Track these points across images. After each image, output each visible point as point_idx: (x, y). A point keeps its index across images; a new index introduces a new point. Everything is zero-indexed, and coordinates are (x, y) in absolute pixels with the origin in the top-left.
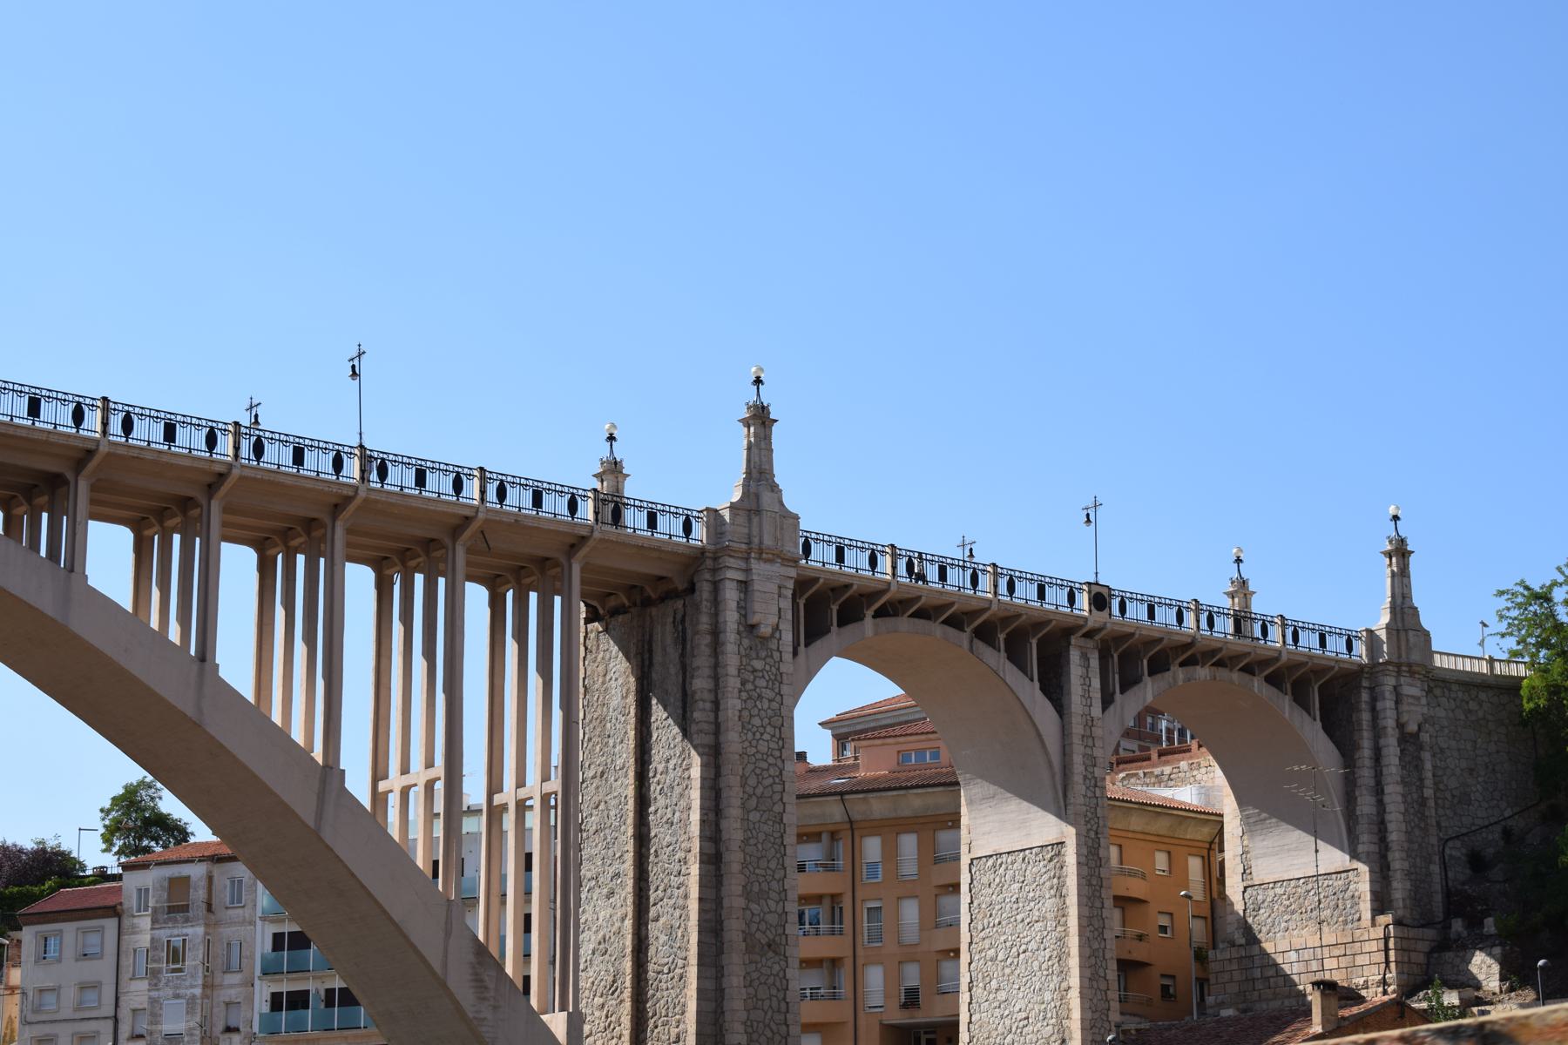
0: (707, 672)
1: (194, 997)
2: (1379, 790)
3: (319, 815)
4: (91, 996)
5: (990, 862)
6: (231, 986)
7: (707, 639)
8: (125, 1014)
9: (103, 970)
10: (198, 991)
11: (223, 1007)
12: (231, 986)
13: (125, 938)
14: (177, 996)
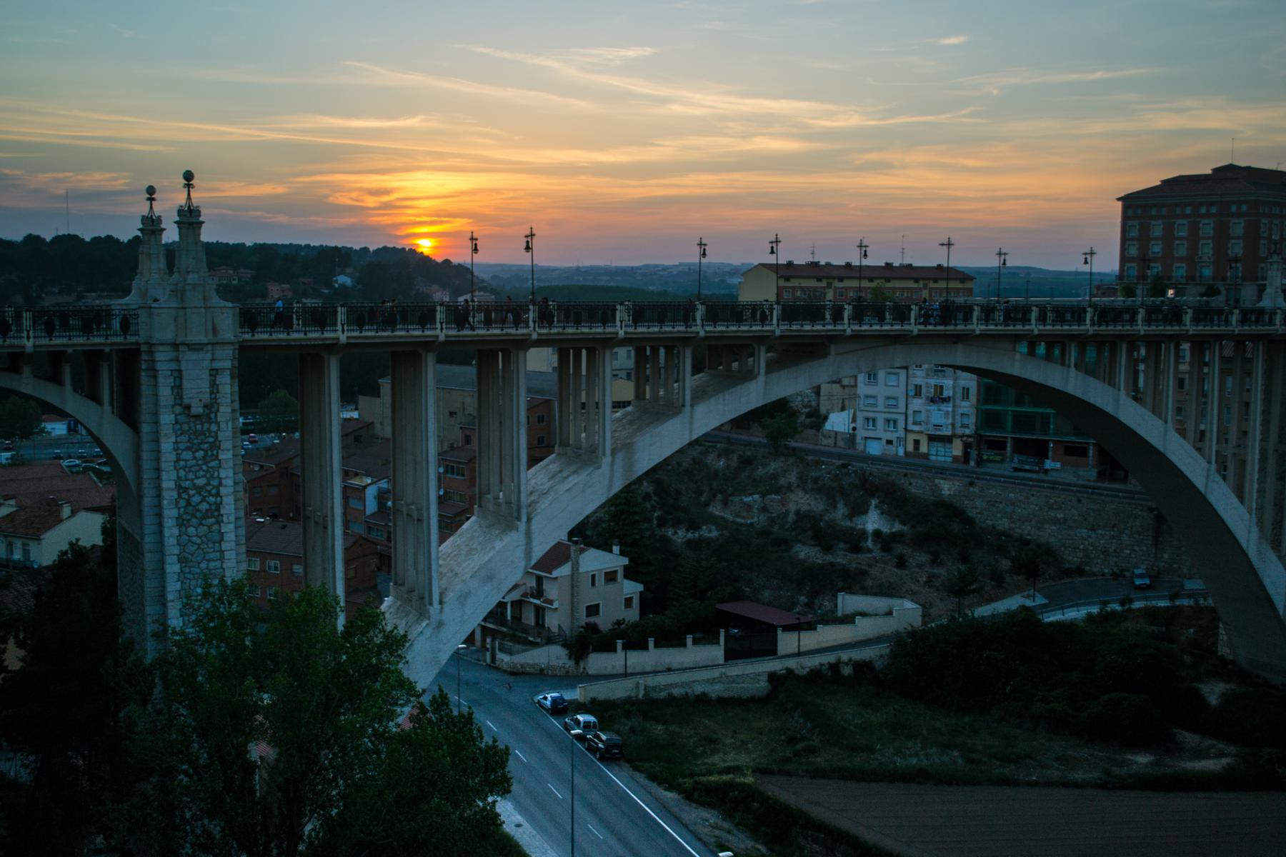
1: (948, 412)
3: (1206, 487)
6: (964, 407)
8: (910, 412)
9: (900, 392)
10: (950, 409)
11: (960, 415)
12: (964, 407)
13: (910, 379)
14: (939, 410)
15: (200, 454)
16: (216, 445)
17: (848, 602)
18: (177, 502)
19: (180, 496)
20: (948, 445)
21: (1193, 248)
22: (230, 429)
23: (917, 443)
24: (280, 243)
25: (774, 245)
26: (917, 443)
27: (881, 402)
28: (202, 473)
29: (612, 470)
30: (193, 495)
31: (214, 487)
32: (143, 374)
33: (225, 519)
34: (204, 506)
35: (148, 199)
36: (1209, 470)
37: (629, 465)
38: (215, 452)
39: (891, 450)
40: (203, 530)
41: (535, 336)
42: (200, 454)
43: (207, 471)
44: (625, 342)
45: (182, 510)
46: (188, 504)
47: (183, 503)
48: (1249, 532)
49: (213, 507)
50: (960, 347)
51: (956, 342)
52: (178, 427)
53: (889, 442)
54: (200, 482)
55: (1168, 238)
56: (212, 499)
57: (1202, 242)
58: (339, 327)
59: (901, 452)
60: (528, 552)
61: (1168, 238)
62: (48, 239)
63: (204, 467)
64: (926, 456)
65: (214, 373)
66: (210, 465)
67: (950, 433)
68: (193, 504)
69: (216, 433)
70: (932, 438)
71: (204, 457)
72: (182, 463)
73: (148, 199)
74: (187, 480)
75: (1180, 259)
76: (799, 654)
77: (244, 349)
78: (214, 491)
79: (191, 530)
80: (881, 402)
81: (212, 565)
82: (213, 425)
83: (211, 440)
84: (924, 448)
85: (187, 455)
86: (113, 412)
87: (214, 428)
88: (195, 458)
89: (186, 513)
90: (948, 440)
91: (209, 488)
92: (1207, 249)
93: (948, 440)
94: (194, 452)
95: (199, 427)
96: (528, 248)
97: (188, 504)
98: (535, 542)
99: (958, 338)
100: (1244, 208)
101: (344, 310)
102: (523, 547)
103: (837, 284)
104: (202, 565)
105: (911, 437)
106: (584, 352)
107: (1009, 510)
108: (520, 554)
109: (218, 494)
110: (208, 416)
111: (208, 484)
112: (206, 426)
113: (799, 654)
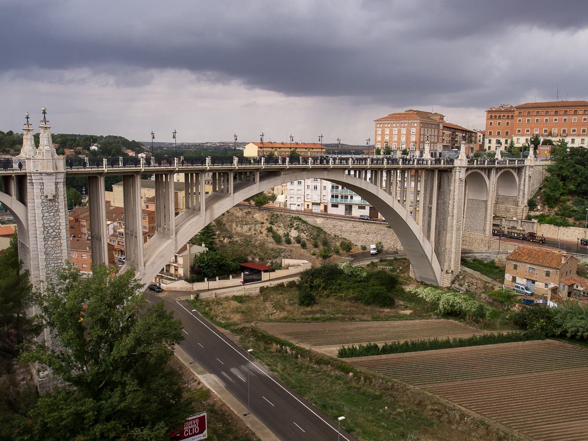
2: (524, 185)
4: (299, 192)
15: (51, 214)
16: (58, 211)
17: (286, 262)
18: (43, 232)
19: (44, 230)
20: (319, 206)
21: (399, 138)
22: (63, 204)
23: (308, 205)
25: (368, 141)
26: (308, 205)
29: (206, 217)
31: (58, 226)
32: (28, 184)
33: (62, 238)
34: (54, 233)
35: (29, 118)
36: (407, 213)
37: (212, 215)
39: (299, 208)
41: (177, 169)
43: (55, 220)
44: (210, 171)
46: (48, 233)
47: (46, 232)
49: (58, 234)
50: (326, 172)
51: (325, 171)
52: (43, 204)
53: (299, 205)
54: (52, 224)
55: (391, 135)
56: (57, 231)
58: (104, 166)
60: (176, 247)
61: (391, 135)
62: (6, 133)
63: (54, 219)
65: (57, 183)
68: (50, 233)
69: (58, 206)
70: (313, 204)
71: (54, 215)
72: (45, 218)
73: (29, 118)
74: (47, 224)
75: (395, 142)
76: (269, 280)
77: (67, 174)
78: (58, 228)
79: (49, 242)
80: (296, 191)
81: (58, 255)
83: (56, 209)
84: (310, 207)
85: (46, 214)
87: (57, 204)
88: (50, 216)
90: (319, 204)
91: (55, 226)
92: (403, 139)
93: (319, 204)
95: (51, 204)
96: (174, 137)
97: (48, 233)
98: (178, 243)
99: (325, 169)
100: (416, 125)
101: (106, 160)
103: (278, 150)
104: (54, 256)
105: (306, 204)
108: (173, 247)
109: (59, 229)
110: (55, 200)
111: (55, 225)
112: (54, 203)
113: (269, 280)
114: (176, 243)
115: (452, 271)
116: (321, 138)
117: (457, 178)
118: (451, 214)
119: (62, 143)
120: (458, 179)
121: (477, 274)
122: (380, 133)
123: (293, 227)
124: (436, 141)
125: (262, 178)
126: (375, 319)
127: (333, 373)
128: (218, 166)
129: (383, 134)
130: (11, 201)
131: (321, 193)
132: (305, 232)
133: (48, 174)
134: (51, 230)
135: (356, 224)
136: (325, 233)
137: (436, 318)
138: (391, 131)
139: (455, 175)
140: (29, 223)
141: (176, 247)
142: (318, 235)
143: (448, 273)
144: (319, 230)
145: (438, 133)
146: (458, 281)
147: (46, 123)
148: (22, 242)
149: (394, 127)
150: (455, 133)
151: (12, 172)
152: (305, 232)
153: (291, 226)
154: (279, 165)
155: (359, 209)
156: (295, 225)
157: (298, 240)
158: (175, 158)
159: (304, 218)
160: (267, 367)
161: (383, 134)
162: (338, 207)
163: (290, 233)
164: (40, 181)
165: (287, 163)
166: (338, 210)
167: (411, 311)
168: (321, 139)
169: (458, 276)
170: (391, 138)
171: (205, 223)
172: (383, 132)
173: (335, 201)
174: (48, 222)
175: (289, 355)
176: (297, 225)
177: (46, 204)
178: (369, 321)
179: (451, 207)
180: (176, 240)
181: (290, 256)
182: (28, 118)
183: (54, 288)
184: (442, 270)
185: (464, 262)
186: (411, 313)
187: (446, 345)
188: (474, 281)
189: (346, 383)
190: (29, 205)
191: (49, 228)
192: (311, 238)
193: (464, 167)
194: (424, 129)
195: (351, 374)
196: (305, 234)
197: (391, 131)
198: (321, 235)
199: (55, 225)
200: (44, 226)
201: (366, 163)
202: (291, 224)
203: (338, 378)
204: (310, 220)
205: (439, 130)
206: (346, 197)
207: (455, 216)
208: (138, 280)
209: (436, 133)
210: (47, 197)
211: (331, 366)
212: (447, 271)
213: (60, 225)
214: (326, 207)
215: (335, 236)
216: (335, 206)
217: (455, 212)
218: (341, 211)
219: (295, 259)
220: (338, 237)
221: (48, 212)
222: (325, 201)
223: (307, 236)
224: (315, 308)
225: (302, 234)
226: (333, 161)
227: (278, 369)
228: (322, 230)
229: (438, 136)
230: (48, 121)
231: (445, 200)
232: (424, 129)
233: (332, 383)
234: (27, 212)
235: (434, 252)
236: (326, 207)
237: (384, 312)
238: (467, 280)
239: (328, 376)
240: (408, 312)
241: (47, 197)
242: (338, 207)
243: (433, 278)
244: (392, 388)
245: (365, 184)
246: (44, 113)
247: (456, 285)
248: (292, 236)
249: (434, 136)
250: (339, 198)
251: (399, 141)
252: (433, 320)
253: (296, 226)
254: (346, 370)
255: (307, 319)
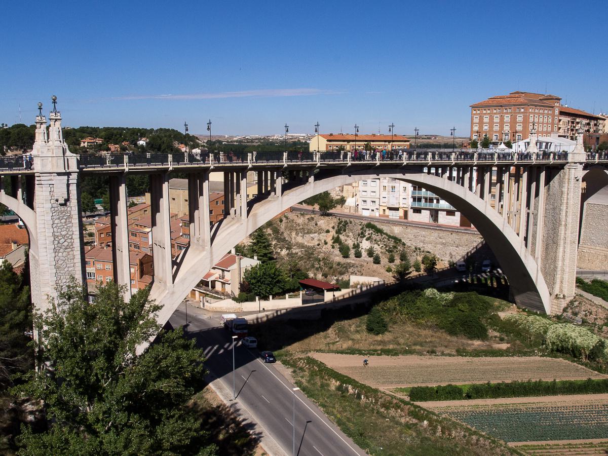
0: (566, 187)
3: (503, 229)
5: (593, 205)
7: (567, 180)
8: (381, 198)
9: (377, 189)
15: (62, 221)
16: (70, 217)
21: (502, 127)
22: (77, 209)
23: (384, 210)
24: (79, 127)
26: (384, 210)
27: (369, 192)
28: (65, 229)
29: (247, 225)
30: (61, 239)
32: (36, 186)
33: (75, 249)
34: (66, 244)
35: (39, 108)
38: (70, 220)
40: (65, 254)
41: (212, 167)
42: (63, 221)
43: (67, 228)
44: (254, 168)
45: (56, 246)
46: (59, 243)
47: (56, 242)
48: (521, 248)
52: (52, 209)
53: (373, 210)
54: (63, 233)
55: (491, 123)
56: (69, 241)
57: (505, 124)
58: (125, 164)
59: (377, 215)
60: (212, 261)
61: (491, 123)
63: (66, 227)
64: (388, 216)
65: (68, 185)
66: (68, 225)
67: (398, 207)
70: (390, 209)
71: (65, 222)
73: (39, 108)
75: (496, 132)
77: (82, 175)
78: (70, 237)
81: (70, 269)
82: (69, 208)
83: (68, 214)
85: (57, 221)
86: (24, 203)
89: (58, 247)
90: (397, 209)
91: (67, 236)
92: (507, 128)
93: (397, 209)
94: (61, 220)
96: (209, 129)
97: (59, 243)
98: (214, 257)
102: (210, 259)
104: (65, 270)
106: (235, 174)
107: (423, 238)
108: (208, 261)
111: (67, 234)
114: (212, 256)
115: (564, 296)
116: (391, 128)
117: (572, 177)
118: (563, 223)
119: (71, 137)
120: (573, 178)
121: (598, 301)
122: (476, 120)
123: (365, 236)
124: (549, 129)
125: (318, 178)
126: (461, 352)
127: (403, 420)
128: (262, 163)
129: (481, 123)
130: (16, 205)
131: (399, 195)
132: (379, 243)
133: (59, 174)
134: (63, 240)
135: (442, 234)
136: (404, 244)
137: (541, 356)
138: (491, 119)
139: (569, 173)
140: (38, 231)
141: (212, 261)
142: (395, 247)
143: (558, 298)
144: (397, 240)
145: (553, 120)
146: (572, 308)
147: (56, 114)
148: (34, 254)
149: (495, 114)
150: (575, 119)
151: (18, 172)
152: (379, 243)
153: (362, 235)
154: (185, 164)
155: (447, 215)
156: (367, 234)
157: (370, 253)
158: (210, 154)
159: (379, 226)
160: (322, 409)
161: (481, 123)
162: (420, 212)
163: (360, 244)
164: (50, 182)
165: (284, 160)
166: (421, 217)
167: (509, 345)
168: (391, 130)
169: (572, 302)
170: (491, 127)
171: (247, 232)
172: (481, 119)
173: (417, 205)
174: (59, 230)
175: (350, 394)
176: (369, 234)
177: (56, 209)
178: (454, 356)
179: (563, 213)
180: (211, 253)
181: (360, 272)
182: (40, 109)
183: (55, 308)
184: (550, 294)
185: (580, 283)
186: (508, 348)
187: (551, 389)
188: (594, 309)
189: (419, 433)
190: (37, 210)
191: (60, 238)
192: (387, 250)
193: (581, 163)
194: (534, 116)
195: (426, 422)
196: (379, 245)
197: (491, 119)
198: (399, 248)
199: (67, 234)
200: (55, 237)
201: (425, 158)
202: (362, 233)
203: (408, 426)
204: (386, 228)
205: (553, 115)
206: (431, 200)
207: (569, 226)
208: (152, 301)
209: (550, 120)
210: (57, 200)
211: (401, 411)
212: (557, 295)
213: (73, 234)
214: (406, 213)
215: (416, 248)
216: (417, 211)
217: (570, 220)
218: (425, 217)
219: (366, 275)
220: (420, 249)
221: (59, 219)
222: (405, 206)
223: (381, 248)
224: (387, 336)
225: (376, 246)
226: (407, 156)
227: (335, 411)
228: (400, 240)
229: (553, 124)
230: (58, 112)
231: (556, 204)
232: (534, 116)
233: (401, 433)
234: (36, 218)
235: (540, 272)
236: (406, 213)
237: (473, 344)
238: (583, 308)
239: (397, 424)
240: (504, 346)
241: (57, 200)
242: (420, 212)
243: (540, 304)
244: (477, 444)
245: (443, 183)
246: (54, 102)
247: (569, 314)
248: (364, 247)
249: (547, 124)
250: (423, 200)
251: (501, 132)
252: (537, 358)
253: (368, 236)
254: (418, 414)
255: (375, 351)
